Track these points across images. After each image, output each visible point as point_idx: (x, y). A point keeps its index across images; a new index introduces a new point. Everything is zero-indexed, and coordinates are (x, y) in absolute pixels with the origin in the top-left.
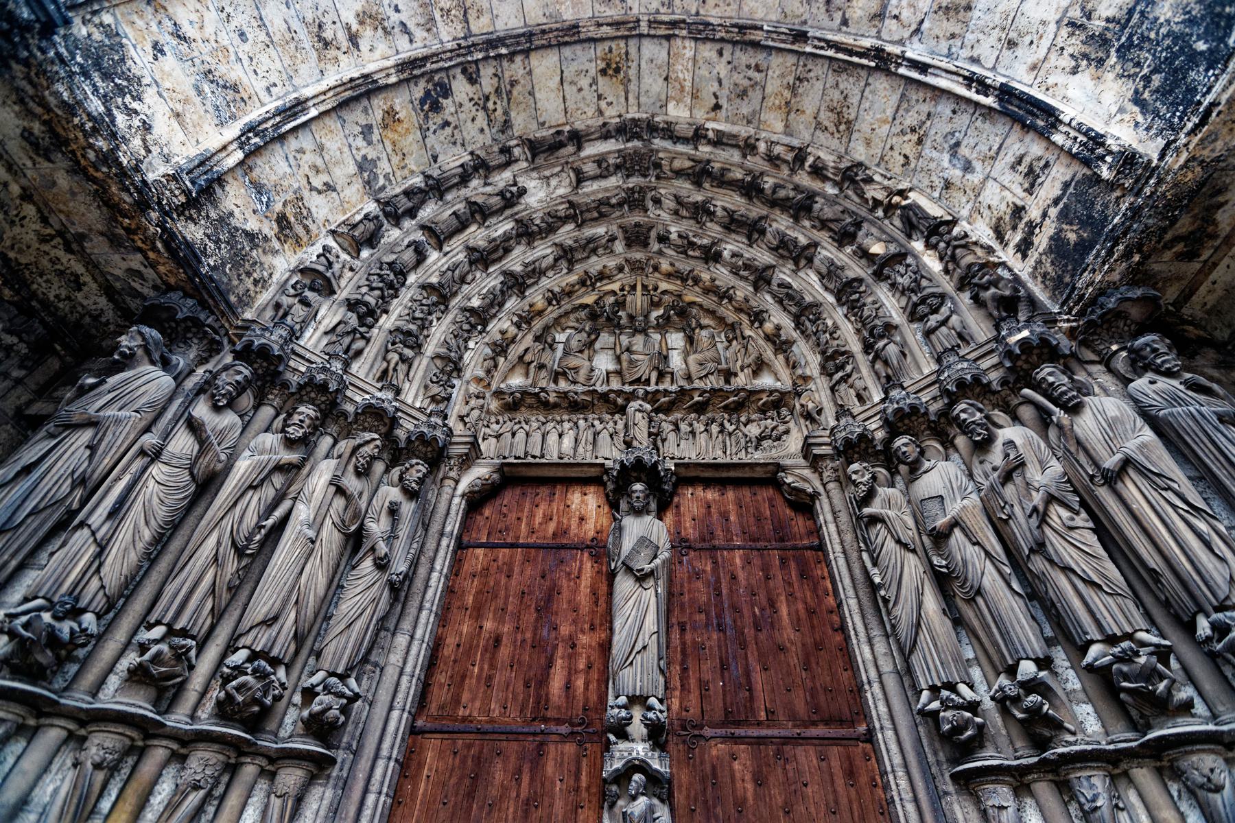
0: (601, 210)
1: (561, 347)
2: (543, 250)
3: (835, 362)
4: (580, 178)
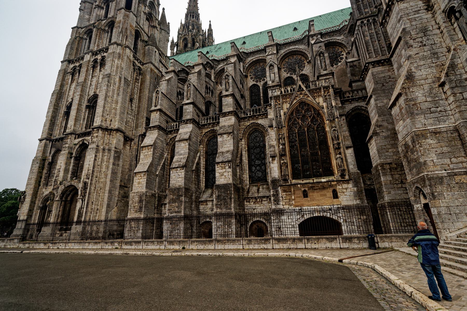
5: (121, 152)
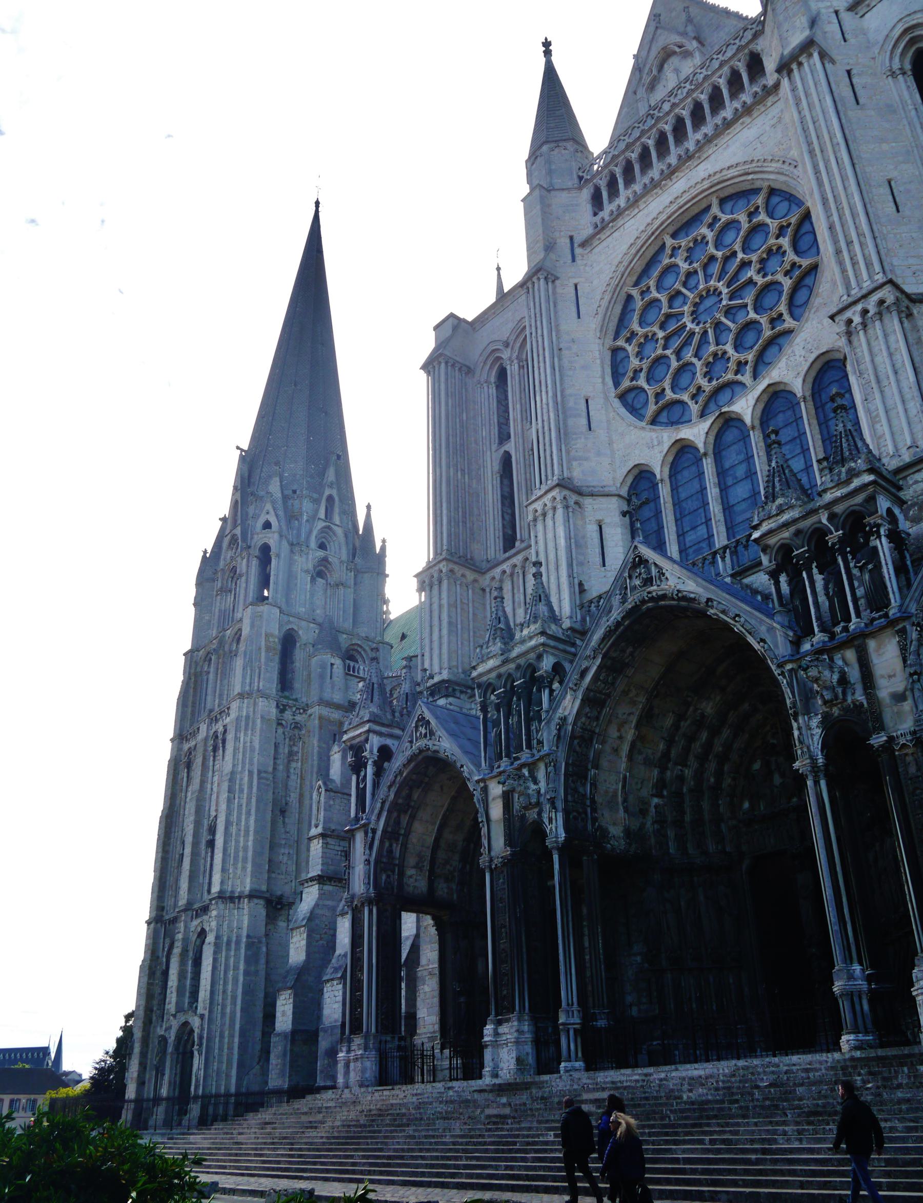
2: (726, 733)
5: (260, 942)
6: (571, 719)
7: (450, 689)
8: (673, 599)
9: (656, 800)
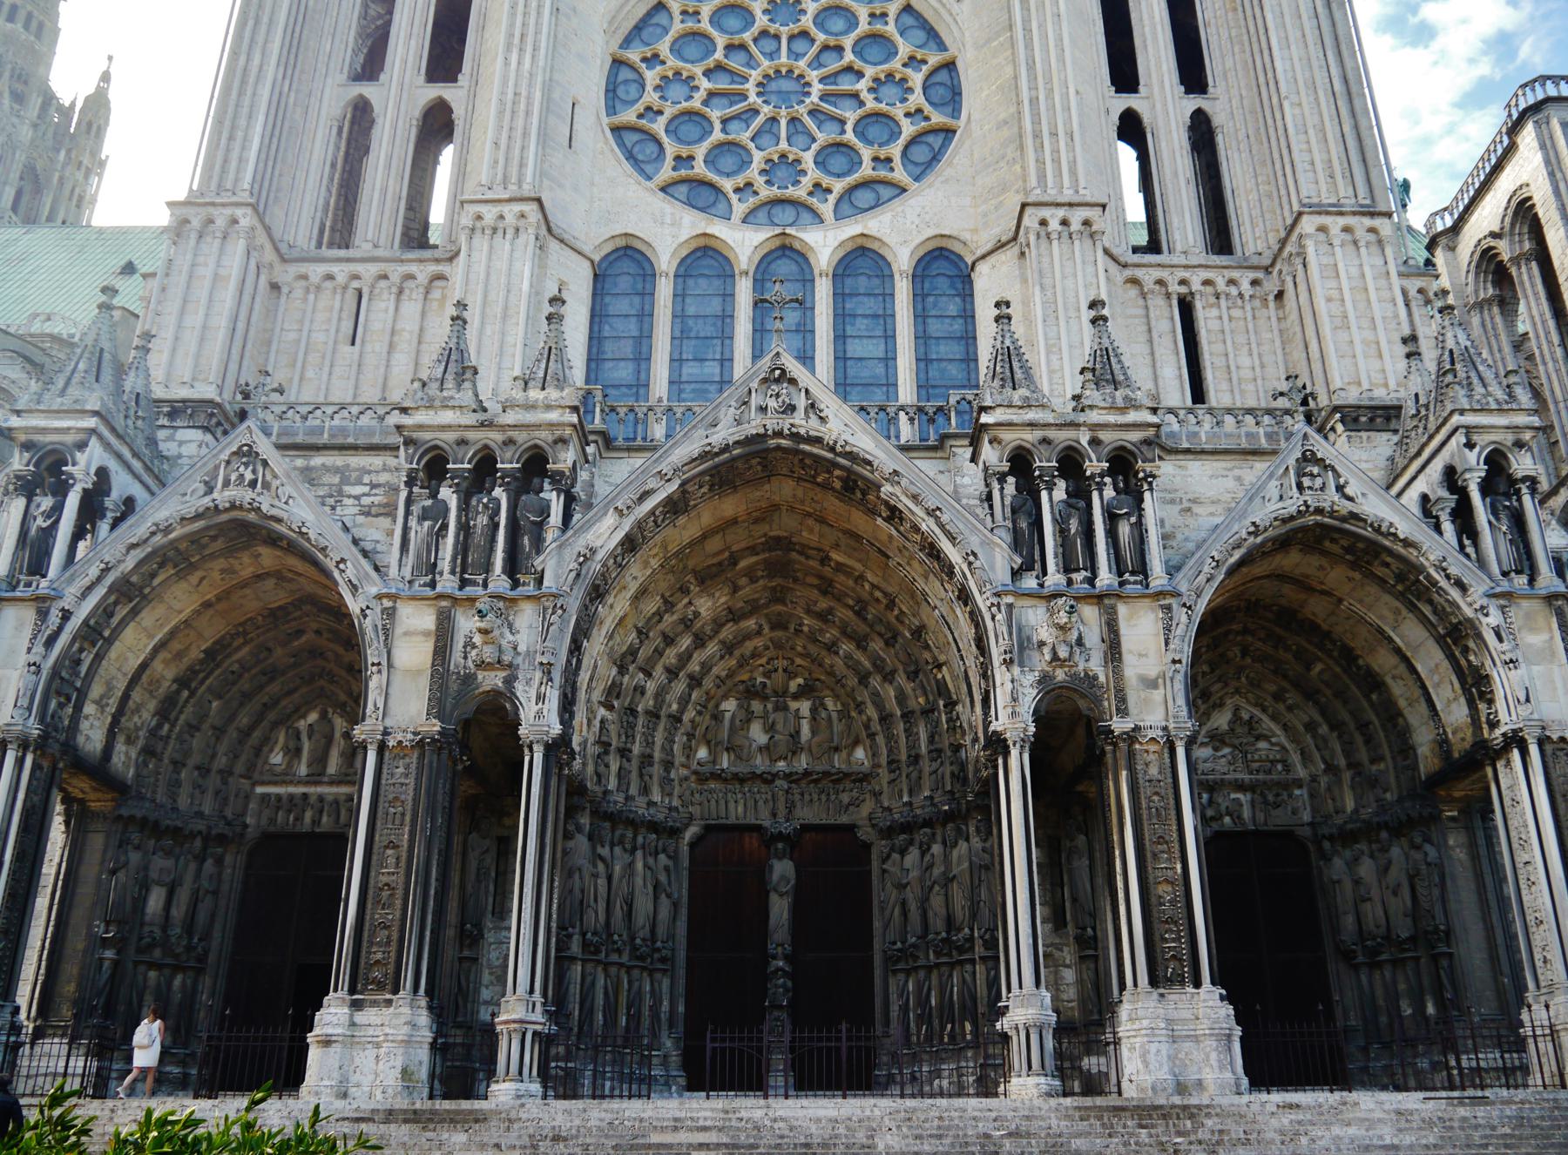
0: (754, 608)
1: (728, 715)
2: (712, 648)
3: (893, 763)
4: (736, 589)
6: (600, 556)
7: (214, 421)
8: (832, 449)
9: (602, 712)
